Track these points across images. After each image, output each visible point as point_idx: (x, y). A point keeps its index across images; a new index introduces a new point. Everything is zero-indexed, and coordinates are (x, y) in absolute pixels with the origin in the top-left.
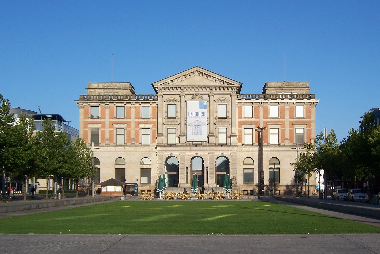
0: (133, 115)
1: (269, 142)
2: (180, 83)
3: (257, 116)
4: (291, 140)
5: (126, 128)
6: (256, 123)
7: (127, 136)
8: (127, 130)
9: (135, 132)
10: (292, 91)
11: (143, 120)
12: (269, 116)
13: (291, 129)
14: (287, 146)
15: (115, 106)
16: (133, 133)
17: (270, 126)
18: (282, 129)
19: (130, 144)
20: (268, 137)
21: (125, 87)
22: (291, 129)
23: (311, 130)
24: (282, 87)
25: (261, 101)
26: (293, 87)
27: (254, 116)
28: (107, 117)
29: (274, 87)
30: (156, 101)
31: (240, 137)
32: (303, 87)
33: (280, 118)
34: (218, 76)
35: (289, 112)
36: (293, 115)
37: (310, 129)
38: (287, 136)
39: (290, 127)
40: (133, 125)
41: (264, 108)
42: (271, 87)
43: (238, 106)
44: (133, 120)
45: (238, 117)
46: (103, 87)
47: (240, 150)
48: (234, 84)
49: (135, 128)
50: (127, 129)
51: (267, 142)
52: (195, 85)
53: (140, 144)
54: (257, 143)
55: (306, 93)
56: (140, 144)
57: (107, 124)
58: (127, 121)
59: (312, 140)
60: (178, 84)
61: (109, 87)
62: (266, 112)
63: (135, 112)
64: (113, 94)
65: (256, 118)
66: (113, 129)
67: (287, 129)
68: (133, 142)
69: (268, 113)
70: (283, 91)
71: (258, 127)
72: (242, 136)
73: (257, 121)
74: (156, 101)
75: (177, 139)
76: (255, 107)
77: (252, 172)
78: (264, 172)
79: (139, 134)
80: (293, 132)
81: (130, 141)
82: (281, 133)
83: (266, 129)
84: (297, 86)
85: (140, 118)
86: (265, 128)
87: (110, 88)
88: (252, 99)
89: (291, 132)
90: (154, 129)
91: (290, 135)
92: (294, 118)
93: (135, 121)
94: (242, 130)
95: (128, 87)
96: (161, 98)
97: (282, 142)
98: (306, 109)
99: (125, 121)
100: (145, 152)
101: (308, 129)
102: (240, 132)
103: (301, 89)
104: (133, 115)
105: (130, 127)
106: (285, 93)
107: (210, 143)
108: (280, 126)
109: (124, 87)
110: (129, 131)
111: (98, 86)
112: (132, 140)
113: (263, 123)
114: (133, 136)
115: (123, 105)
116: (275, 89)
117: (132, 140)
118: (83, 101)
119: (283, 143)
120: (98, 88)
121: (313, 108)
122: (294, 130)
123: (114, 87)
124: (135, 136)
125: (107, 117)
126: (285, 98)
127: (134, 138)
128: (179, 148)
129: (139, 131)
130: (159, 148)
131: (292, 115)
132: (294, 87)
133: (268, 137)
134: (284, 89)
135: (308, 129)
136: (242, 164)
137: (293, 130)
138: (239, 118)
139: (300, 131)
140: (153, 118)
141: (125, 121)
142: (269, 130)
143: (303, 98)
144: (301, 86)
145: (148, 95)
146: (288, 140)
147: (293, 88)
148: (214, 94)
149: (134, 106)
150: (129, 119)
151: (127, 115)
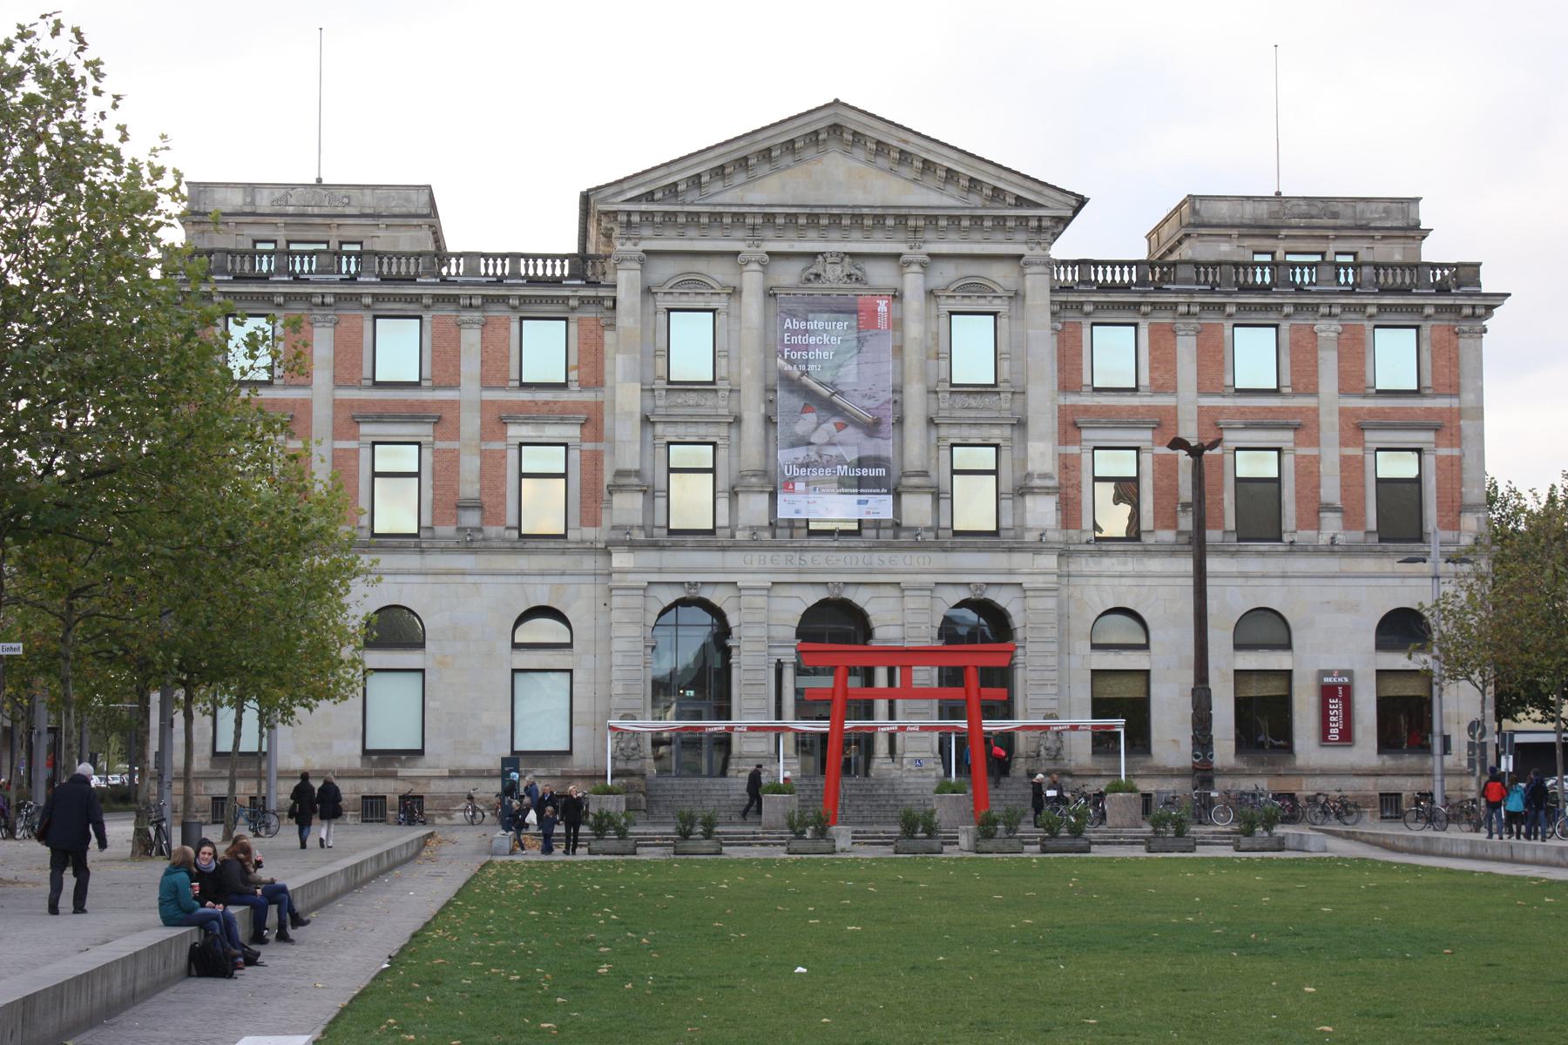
0: (470, 365)
2: (738, 190)
3: (1165, 382)
4: (1351, 516)
5: (431, 439)
6: (1160, 422)
7: (435, 488)
8: (436, 452)
9: (482, 463)
10: (1331, 248)
11: (525, 396)
12: (1228, 381)
13: (1349, 451)
15: (368, 315)
16: (470, 465)
17: (1232, 438)
18: (1302, 451)
19: (454, 528)
21: (404, 210)
22: (1349, 451)
23: (1460, 459)
24: (1272, 222)
25: (1188, 300)
26: (1331, 222)
27: (1145, 380)
28: (322, 376)
29: (1229, 221)
30: (602, 292)
32: (1389, 224)
33: (1289, 390)
34: (955, 156)
36: (1361, 376)
37: (1456, 452)
38: (1330, 491)
39: (1344, 443)
40: (470, 424)
41: (1201, 336)
42: (1214, 221)
43: (1060, 327)
44: (470, 391)
45: (1059, 385)
46: (277, 209)
48: (1040, 201)
49: (482, 439)
50: (440, 445)
52: (826, 206)
53: (508, 528)
55: (1404, 257)
56: (508, 528)
57: (322, 416)
58: (435, 402)
59: (1468, 515)
60: (727, 197)
61: (309, 210)
62: (1215, 360)
63: (484, 349)
64: (334, 246)
65: (1158, 389)
66: (352, 444)
67: (1330, 456)
68: (471, 519)
69: (1221, 363)
70: (1280, 249)
71: (1177, 443)
72: (1080, 492)
73: (1166, 408)
74: (602, 292)
75: (723, 505)
76: (1150, 332)
77: (1143, 696)
78: (1210, 690)
79: (505, 476)
80: (1364, 471)
81: (454, 511)
82: (1296, 472)
83: (1217, 451)
84: (1355, 219)
85: (511, 384)
86: (1213, 446)
87: (316, 211)
88: (1133, 288)
89: (1352, 469)
90: (588, 446)
91: (1345, 487)
92: (1365, 396)
93: (482, 402)
94: (1079, 457)
95: (420, 211)
96: (632, 272)
98: (1433, 346)
99: (423, 403)
100: (538, 579)
101: (1444, 452)
102: (1068, 465)
103: (1378, 234)
104: (470, 365)
105: (455, 434)
106: (1290, 258)
107: (909, 529)
108: (1289, 435)
109: (397, 211)
110: (449, 455)
111: (245, 204)
112: (463, 506)
113: (1196, 417)
114: (469, 487)
115: (411, 308)
116: (1235, 232)
117: (463, 506)
118: (284, 282)
119: (1310, 527)
120: (247, 209)
121: (1470, 337)
122: (1369, 458)
123: (339, 210)
124: (482, 488)
125: (322, 376)
126: (1218, 279)
127: (477, 495)
128: (734, 559)
129: (504, 457)
130: (621, 559)
131: (1355, 378)
132: (1339, 222)
133: (1225, 494)
134: (1284, 232)
135: (1444, 452)
137: (1362, 461)
139: (1400, 467)
140: (584, 386)
141: (425, 398)
142: (1229, 458)
143: (1415, 281)
144: (1380, 219)
145: (554, 257)
146: (1338, 515)
147: (1335, 228)
148: (927, 259)
149: (477, 315)
150: (450, 387)
151: (434, 364)
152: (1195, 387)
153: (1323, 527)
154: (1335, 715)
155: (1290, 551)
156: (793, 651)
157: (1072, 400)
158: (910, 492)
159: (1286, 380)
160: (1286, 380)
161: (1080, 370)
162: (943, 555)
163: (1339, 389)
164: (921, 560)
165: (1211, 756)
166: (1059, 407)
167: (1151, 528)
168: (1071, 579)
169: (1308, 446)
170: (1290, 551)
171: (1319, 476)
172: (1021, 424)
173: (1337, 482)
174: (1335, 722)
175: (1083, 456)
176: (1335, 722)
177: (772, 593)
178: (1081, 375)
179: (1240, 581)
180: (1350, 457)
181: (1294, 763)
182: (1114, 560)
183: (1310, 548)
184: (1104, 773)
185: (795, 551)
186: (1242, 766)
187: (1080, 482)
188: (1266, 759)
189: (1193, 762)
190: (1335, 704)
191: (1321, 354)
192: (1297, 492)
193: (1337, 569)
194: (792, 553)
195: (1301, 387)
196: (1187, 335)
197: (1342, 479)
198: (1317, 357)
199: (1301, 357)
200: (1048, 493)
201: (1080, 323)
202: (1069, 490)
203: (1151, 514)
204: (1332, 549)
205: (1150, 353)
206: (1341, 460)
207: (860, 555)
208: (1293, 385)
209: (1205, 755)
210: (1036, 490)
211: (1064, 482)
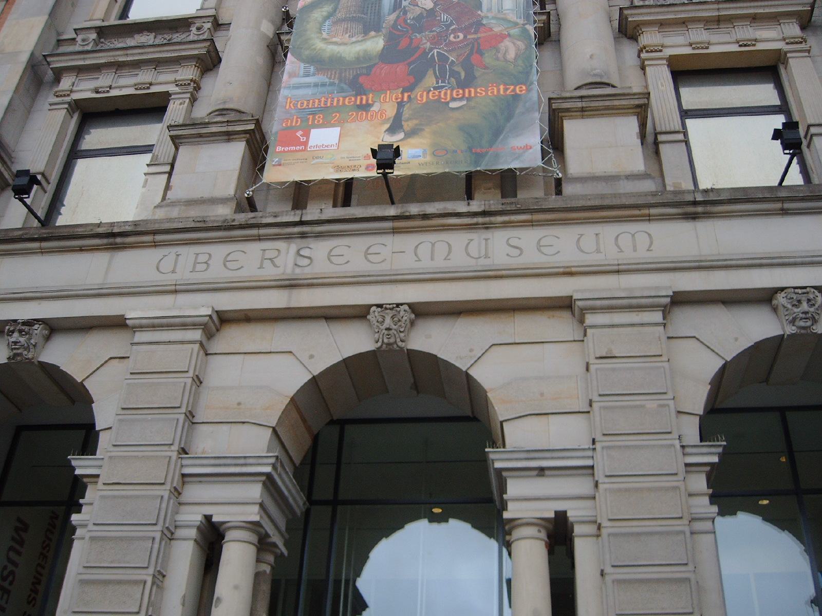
156: (255, 491)
158: (583, 112)
162: (684, 229)
164: (625, 241)
177: (218, 345)
185: (289, 237)
194: (281, 245)
207: (458, 239)
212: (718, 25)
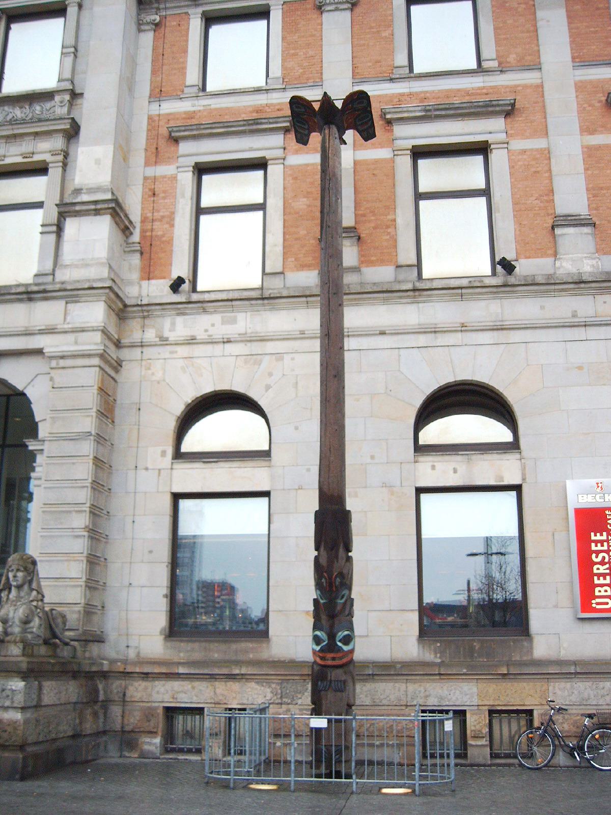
1: (407, 255)
14: (579, 284)
18: (518, 144)
20: (404, 216)
31: (159, 228)
33: (494, 64)
35: (571, 18)
47: (150, 335)
51: (388, 255)
54: (303, 267)
72: (172, 226)
94: (174, 178)
97: (526, 248)
108: (498, 123)
119: (540, 253)
133: (398, 211)
136: (164, 453)
138: (158, 94)
146: (586, 230)
152: (350, 74)
153: (561, 250)
154: (602, 563)
155: (505, 286)
157: (170, 107)
159: (489, 51)
160: (489, 51)
161: (183, 70)
163: (573, 58)
165: (347, 640)
166: (150, 118)
167: (280, 270)
168: (145, 350)
169: (527, 138)
170: (505, 286)
171: (550, 178)
172: (73, 132)
173: (580, 183)
174: (604, 576)
175: (180, 176)
176: (604, 576)
178: (184, 74)
179: (422, 340)
180: (598, 148)
181: (532, 653)
182: (217, 318)
183: (540, 280)
184: (181, 670)
186: (429, 656)
187: (173, 213)
188: (477, 645)
189: (314, 652)
190: (602, 542)
191: (540, 14)
192: (515, 203)
193: (591, 312)
195: (512, 58)
196: (337, 9)
197: (588, 179)
198: (535, 19)
199: (510, 22)
200: (97, 212)
201: (187, 13)
202: (157, 225)
203: (279, 249)
204: (579, 284)
205: (283, 39)
206: (583, 153)
208: (500, 58)
209: (332, 636)
210: (78, 208)
211: (149, 215)
212: (15, 139)
